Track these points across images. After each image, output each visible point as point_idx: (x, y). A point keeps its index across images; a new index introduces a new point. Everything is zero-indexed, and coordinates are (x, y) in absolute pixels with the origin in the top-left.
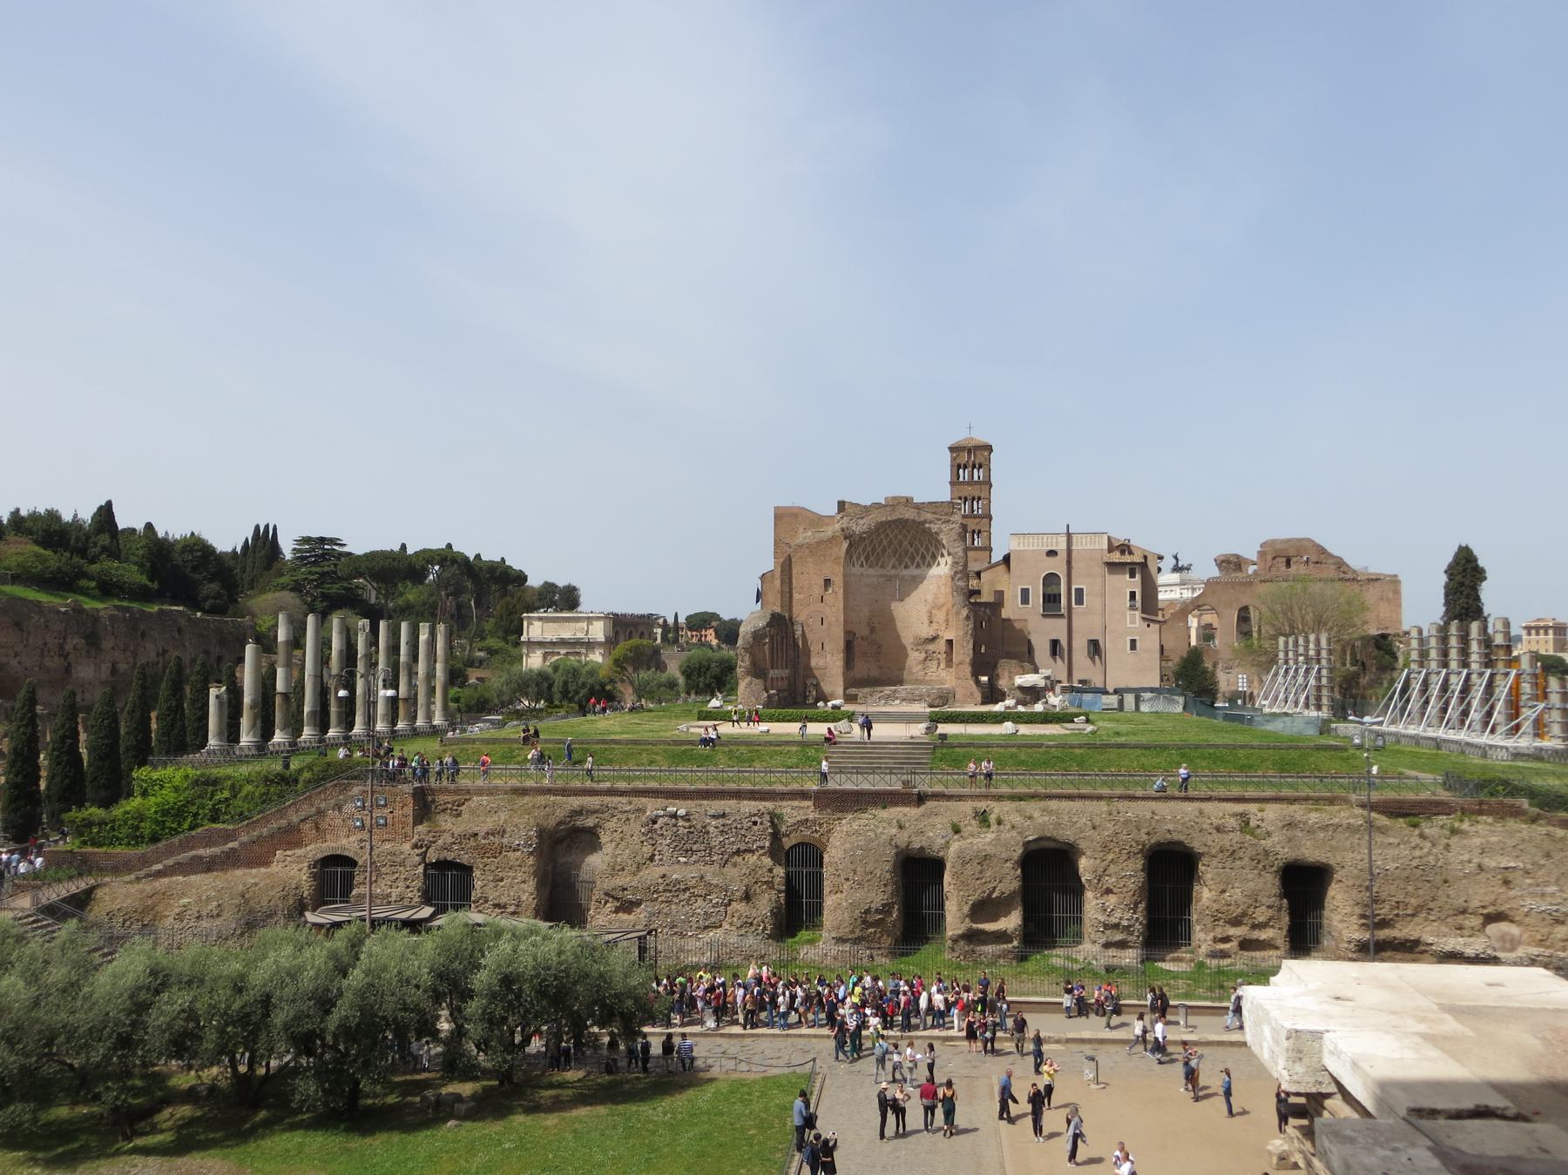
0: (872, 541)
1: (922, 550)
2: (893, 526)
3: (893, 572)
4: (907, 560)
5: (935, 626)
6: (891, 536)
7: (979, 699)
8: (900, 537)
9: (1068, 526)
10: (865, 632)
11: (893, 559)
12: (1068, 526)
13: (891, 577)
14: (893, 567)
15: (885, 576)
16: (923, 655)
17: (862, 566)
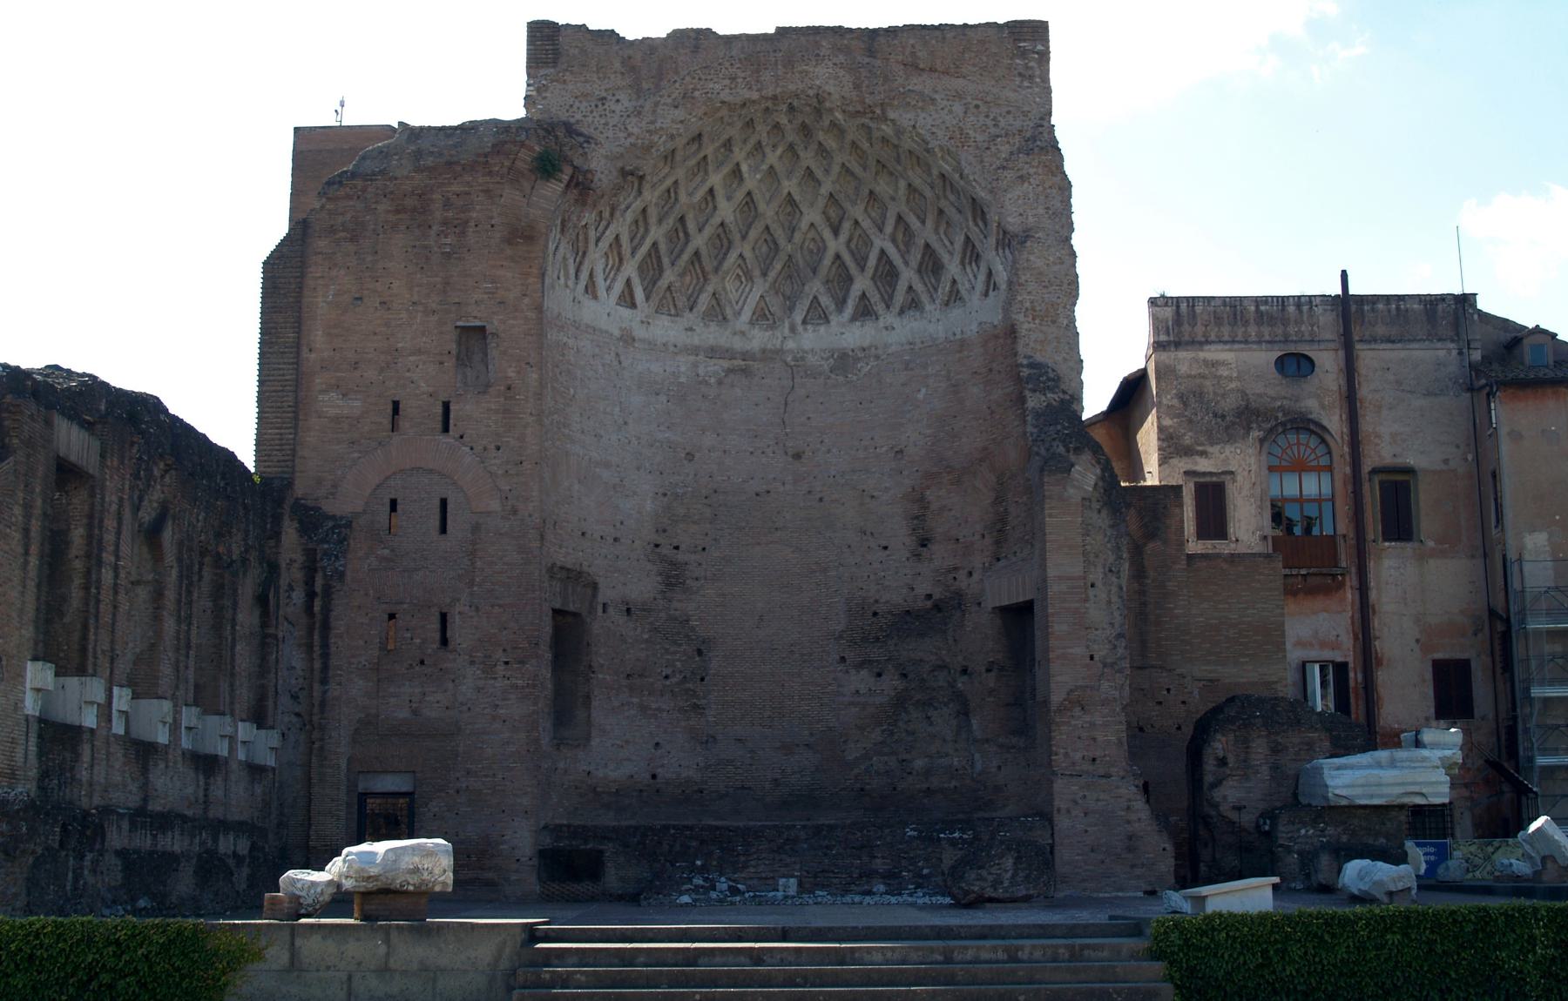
0: (671, 194)
1: (880, 242)
2: (762, 131)
3: (759, 339)
4: (815, 287)
5: (941, 555)
6: (752, 181)
7: (1167, 865)
8: (790, 185)
9: (1344, 275)
10: (642, 585)
11: (759, 288)
12: (1344, 275)
13: (745, 356)
14: (762, 316)
15: (728, 353)
16: (890, 683)
17: (628, 300)
